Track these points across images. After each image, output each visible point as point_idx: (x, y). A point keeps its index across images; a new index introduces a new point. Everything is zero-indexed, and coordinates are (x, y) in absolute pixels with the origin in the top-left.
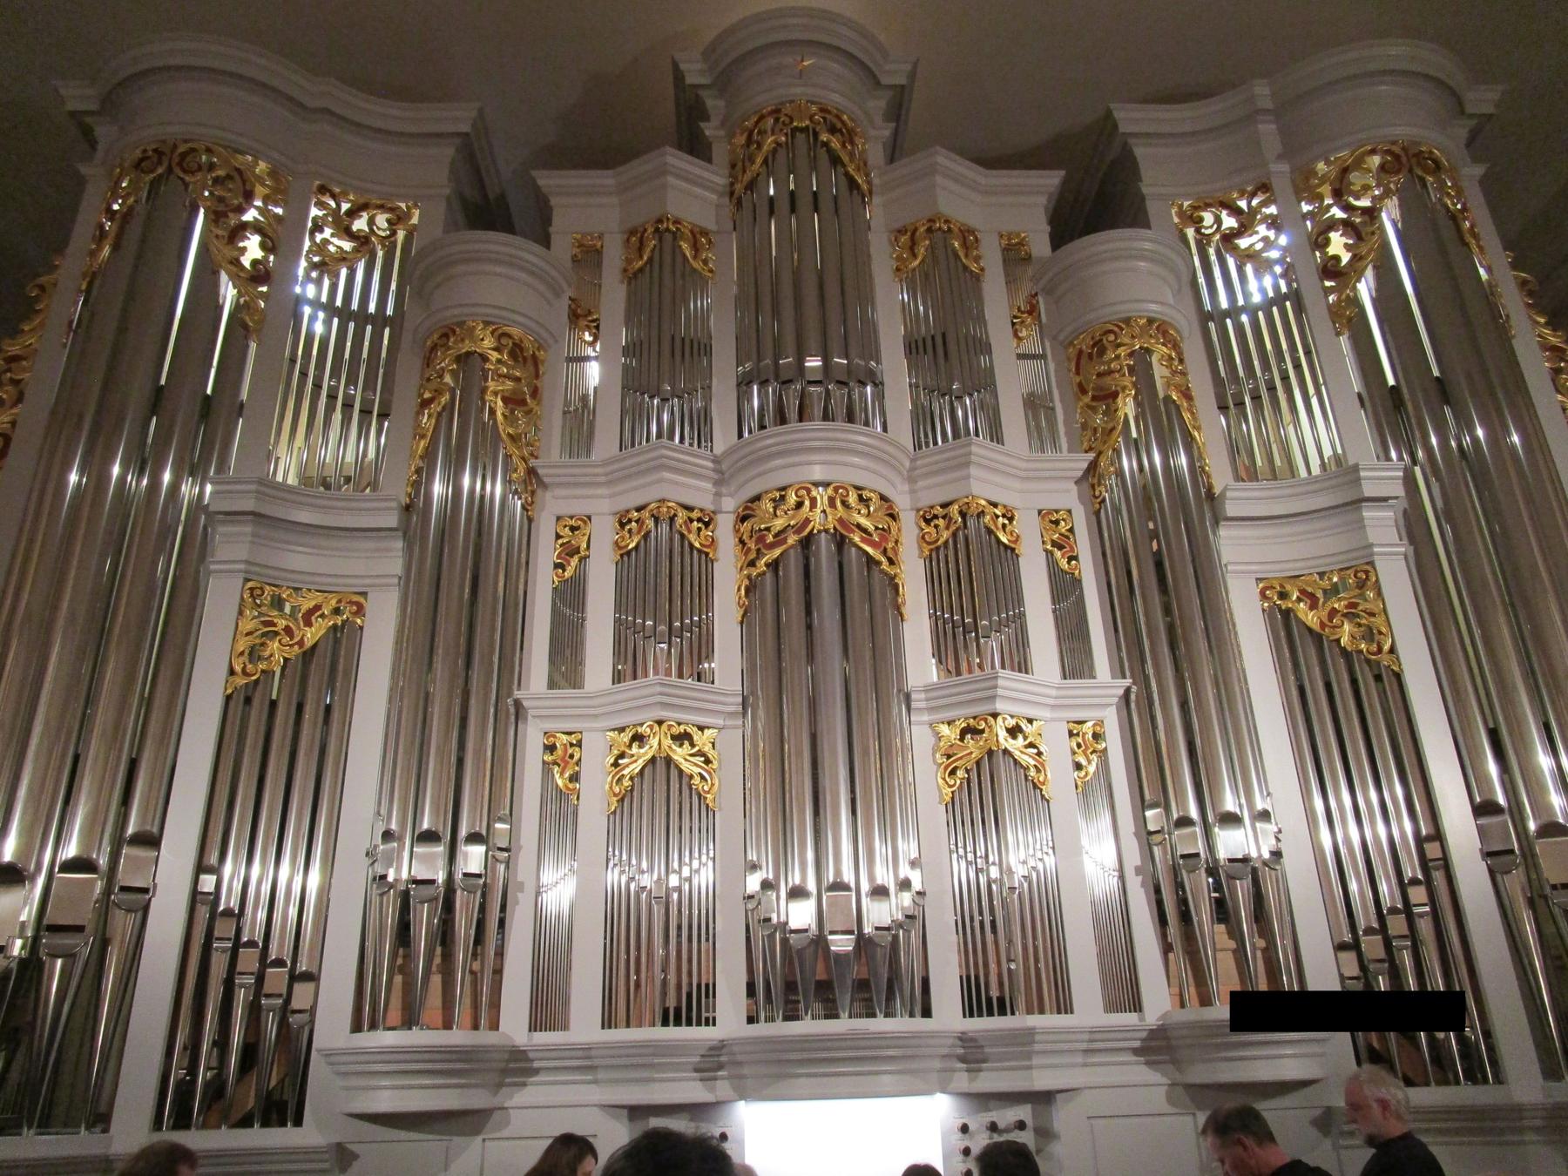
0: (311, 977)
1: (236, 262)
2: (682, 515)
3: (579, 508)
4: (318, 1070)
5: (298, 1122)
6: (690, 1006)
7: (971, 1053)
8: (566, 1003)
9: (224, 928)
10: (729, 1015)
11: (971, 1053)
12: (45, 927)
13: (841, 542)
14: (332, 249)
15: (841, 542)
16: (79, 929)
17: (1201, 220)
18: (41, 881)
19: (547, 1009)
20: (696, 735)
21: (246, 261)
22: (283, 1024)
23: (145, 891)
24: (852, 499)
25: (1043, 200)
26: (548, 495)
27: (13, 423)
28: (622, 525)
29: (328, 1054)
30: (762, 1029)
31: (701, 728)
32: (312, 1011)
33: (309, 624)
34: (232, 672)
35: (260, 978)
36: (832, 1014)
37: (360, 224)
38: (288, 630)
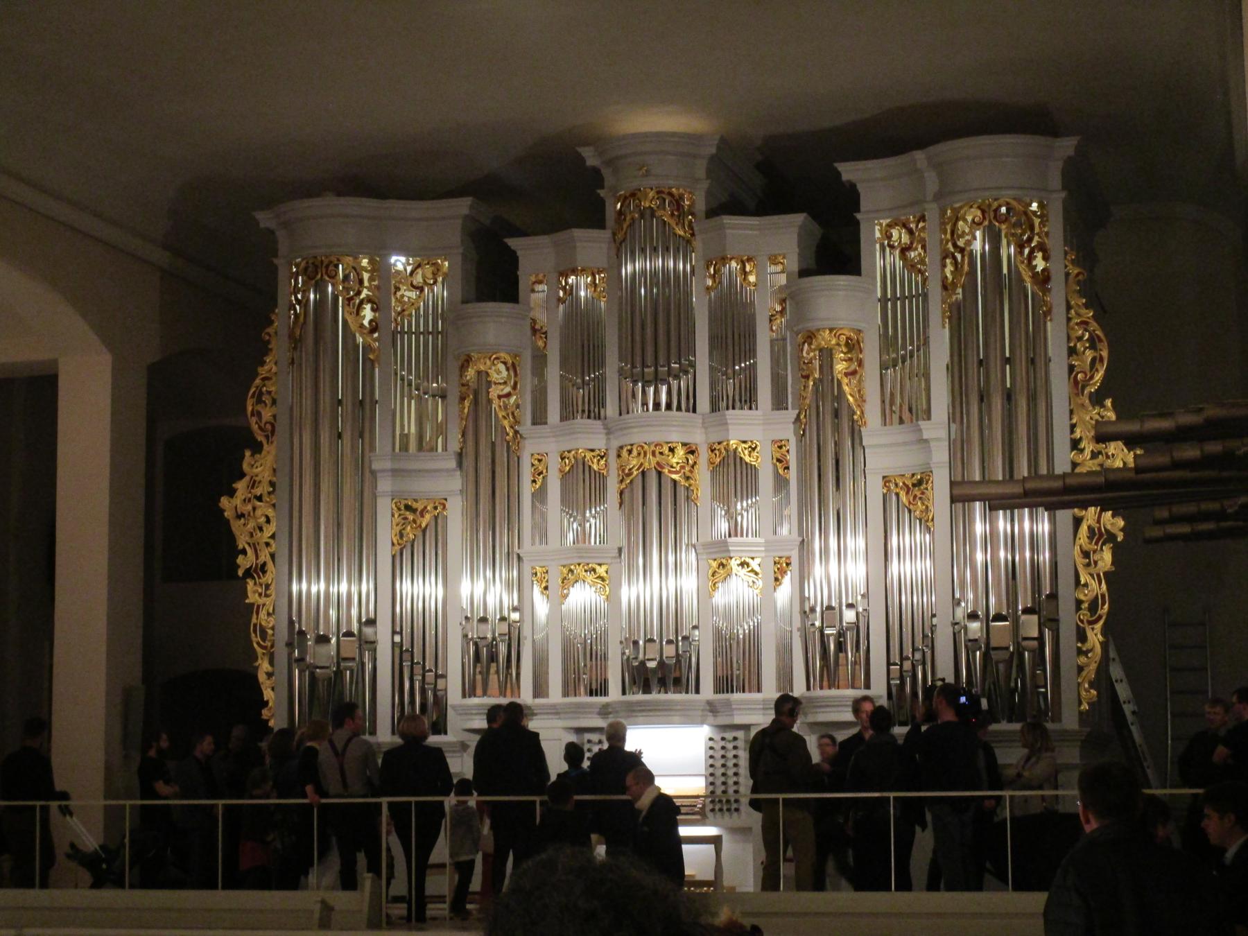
0: (444, 676)
1: (362, 326)
2: (589, 455)
3: (543, 449)
4: (451, 714)
5: (446, 733)
6: (602, 690)
7: (712, 708)
8: (548, 687)
9: (406, 656)
10: (614, 693)
11: (712, 708)
12: (340, 659)
13: (660, 474)
14: (406, 299)
15: (660, 474)
16: (354, 659)
17: (891, 235)
18: (334, 641)
19: (540, 689)
20: (598, 568)
21: (366, 322)
22: (435, 696)
23: (373, 642)
24: (667, 452)
25: (796, 230)
26: (527, 442)
27: (274, 416)
28: (563, 459)
29: (453, 707)
30: (629, 697)
31: (600, 565)
32: (446, 690)
33: (422, 516)
34: (393, 544)
35: (424, 676)
36: (666, 692)
37: (418, 279)
38: (414, 521)
